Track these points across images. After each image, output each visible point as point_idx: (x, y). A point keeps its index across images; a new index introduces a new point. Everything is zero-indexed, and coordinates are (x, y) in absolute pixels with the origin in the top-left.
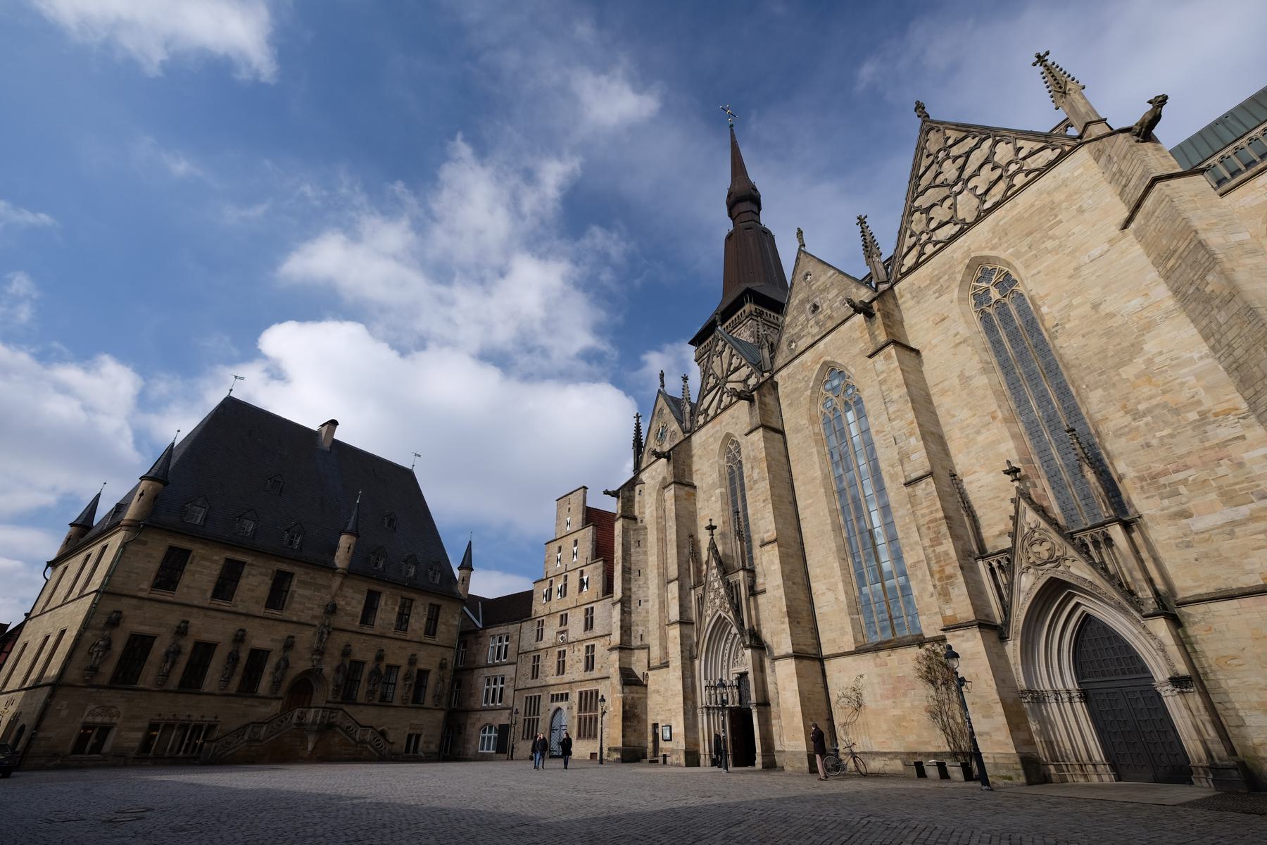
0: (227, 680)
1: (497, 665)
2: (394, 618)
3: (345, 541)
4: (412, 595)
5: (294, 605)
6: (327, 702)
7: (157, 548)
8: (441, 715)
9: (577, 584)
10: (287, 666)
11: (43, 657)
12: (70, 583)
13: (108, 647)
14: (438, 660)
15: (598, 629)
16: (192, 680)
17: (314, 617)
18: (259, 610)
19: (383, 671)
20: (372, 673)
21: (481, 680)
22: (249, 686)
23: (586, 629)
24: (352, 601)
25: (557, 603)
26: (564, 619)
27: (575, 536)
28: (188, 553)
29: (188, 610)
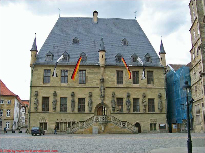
0: (73, 109)
4: (137, 70)
5: (88, 81)
6: (111, 114)
7: (41, 71)
10: (92, 103)
13: (38, 101)
14: (158, 94)
16: (64, 109)
17: (97, 84)
19: (132, 101)
20: (127, 102)
22: (82, 109)
24: (111, 76)
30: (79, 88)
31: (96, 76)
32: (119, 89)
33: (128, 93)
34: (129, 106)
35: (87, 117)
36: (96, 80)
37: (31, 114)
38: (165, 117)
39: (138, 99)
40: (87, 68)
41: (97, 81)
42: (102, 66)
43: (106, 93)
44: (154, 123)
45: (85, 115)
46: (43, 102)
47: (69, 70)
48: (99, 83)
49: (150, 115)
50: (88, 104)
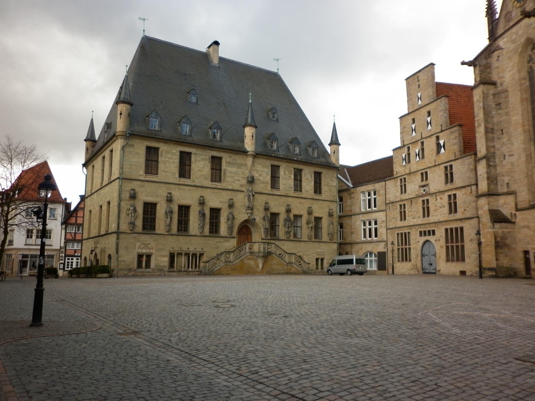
1: (370, 212)
2: (291, 183)
3: (249, 132)
4: (300, 167)
5: (227, 179)
8: (335, 246)
9: (434, 147)
10: (234, 218)
11: (104, 218)
12: (100, 175)
13: (135, 210)
14: (327, 210)
15: (458, 181)
17: (242, 186)
18: (208, 183)
19: (292, 219)
21: (358, 223)
23: (447, 182)
25: (416, 164)
26: (425, 176)
27: (428, 108)
28: (157, 149)
29: (169, 186)
30: (212, 190)
32: (275, 197)
33: (287, 205)
35: (224, 244)
36: (238, 178)
37: (122, 236)
38: (336, 249)
39: (301, 216)
40: (226, 154)
41: (241, 179)
42: (252, 153)
43: (255, 203)
44: (322, 257)
45: (222, 240)
46: (145, 212)
47: (195, 154)
48: (243, 183)
49: (317, 244)
50: (226, 221)
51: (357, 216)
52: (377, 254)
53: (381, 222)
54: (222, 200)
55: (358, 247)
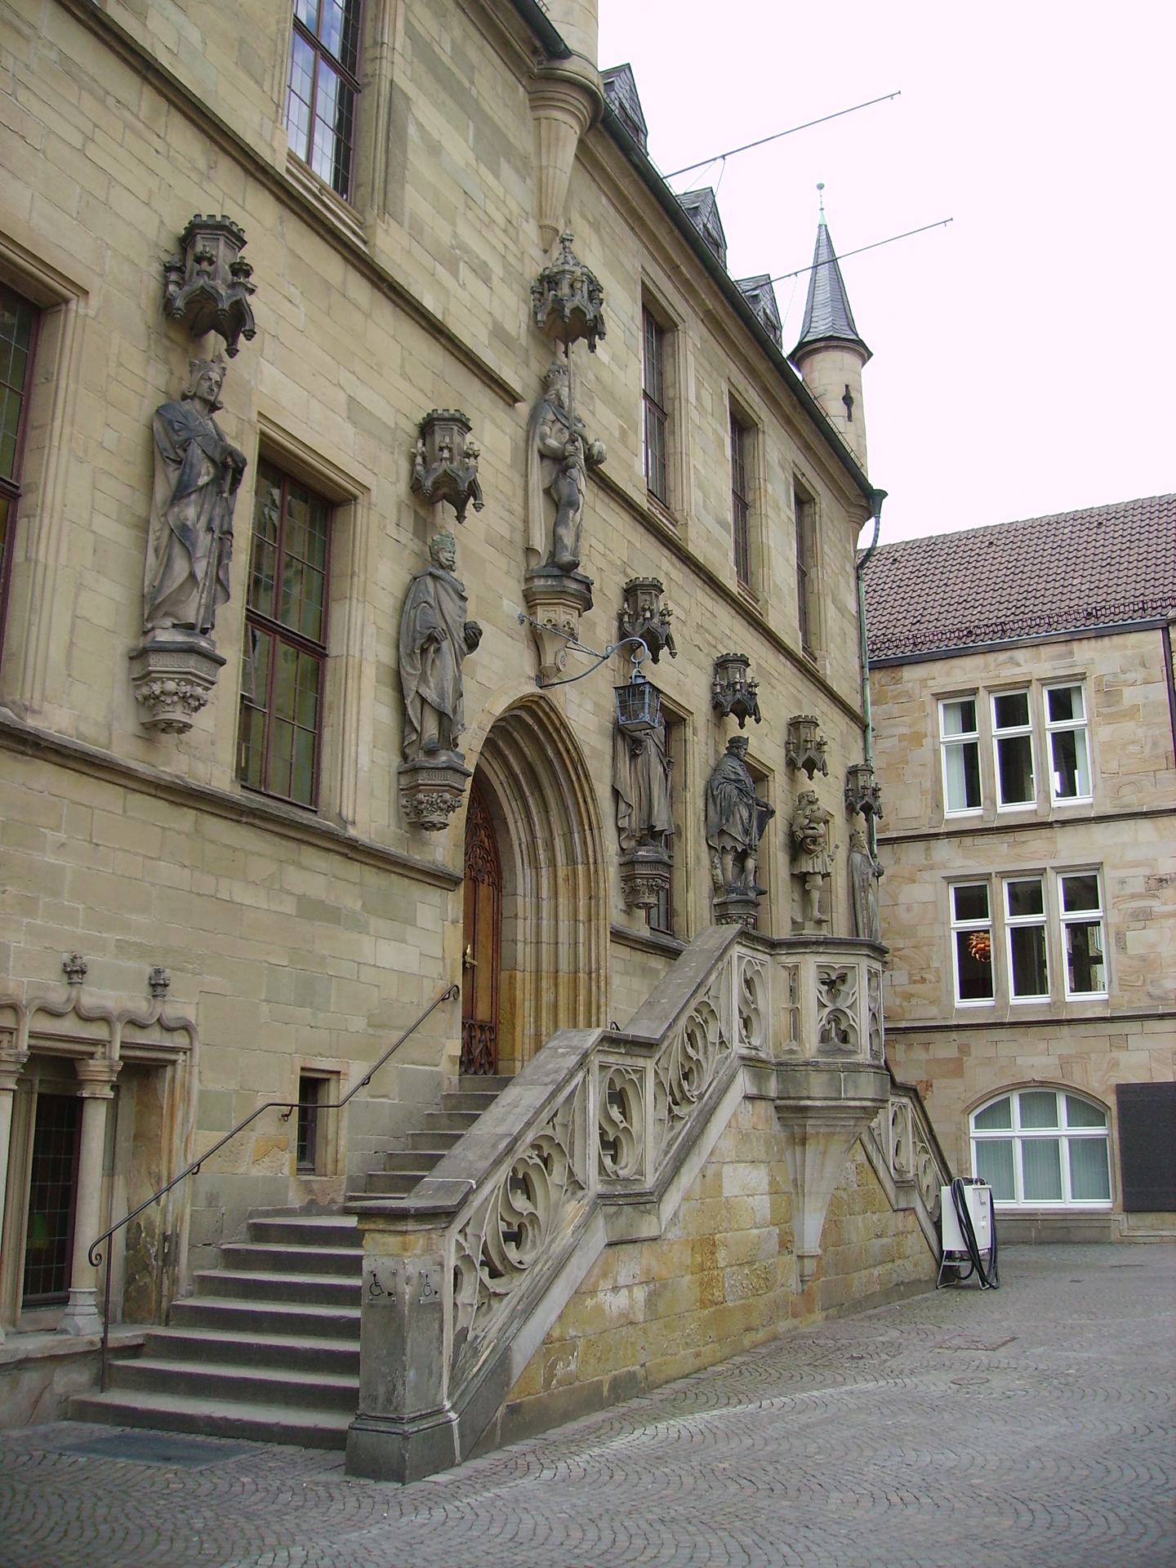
31: (483, 170)
34: (741, 858)
51: (914, 854)
52: (1111, 1101)
53: (1138, 886)
54: (365, 397)
55: (919, 1054)
